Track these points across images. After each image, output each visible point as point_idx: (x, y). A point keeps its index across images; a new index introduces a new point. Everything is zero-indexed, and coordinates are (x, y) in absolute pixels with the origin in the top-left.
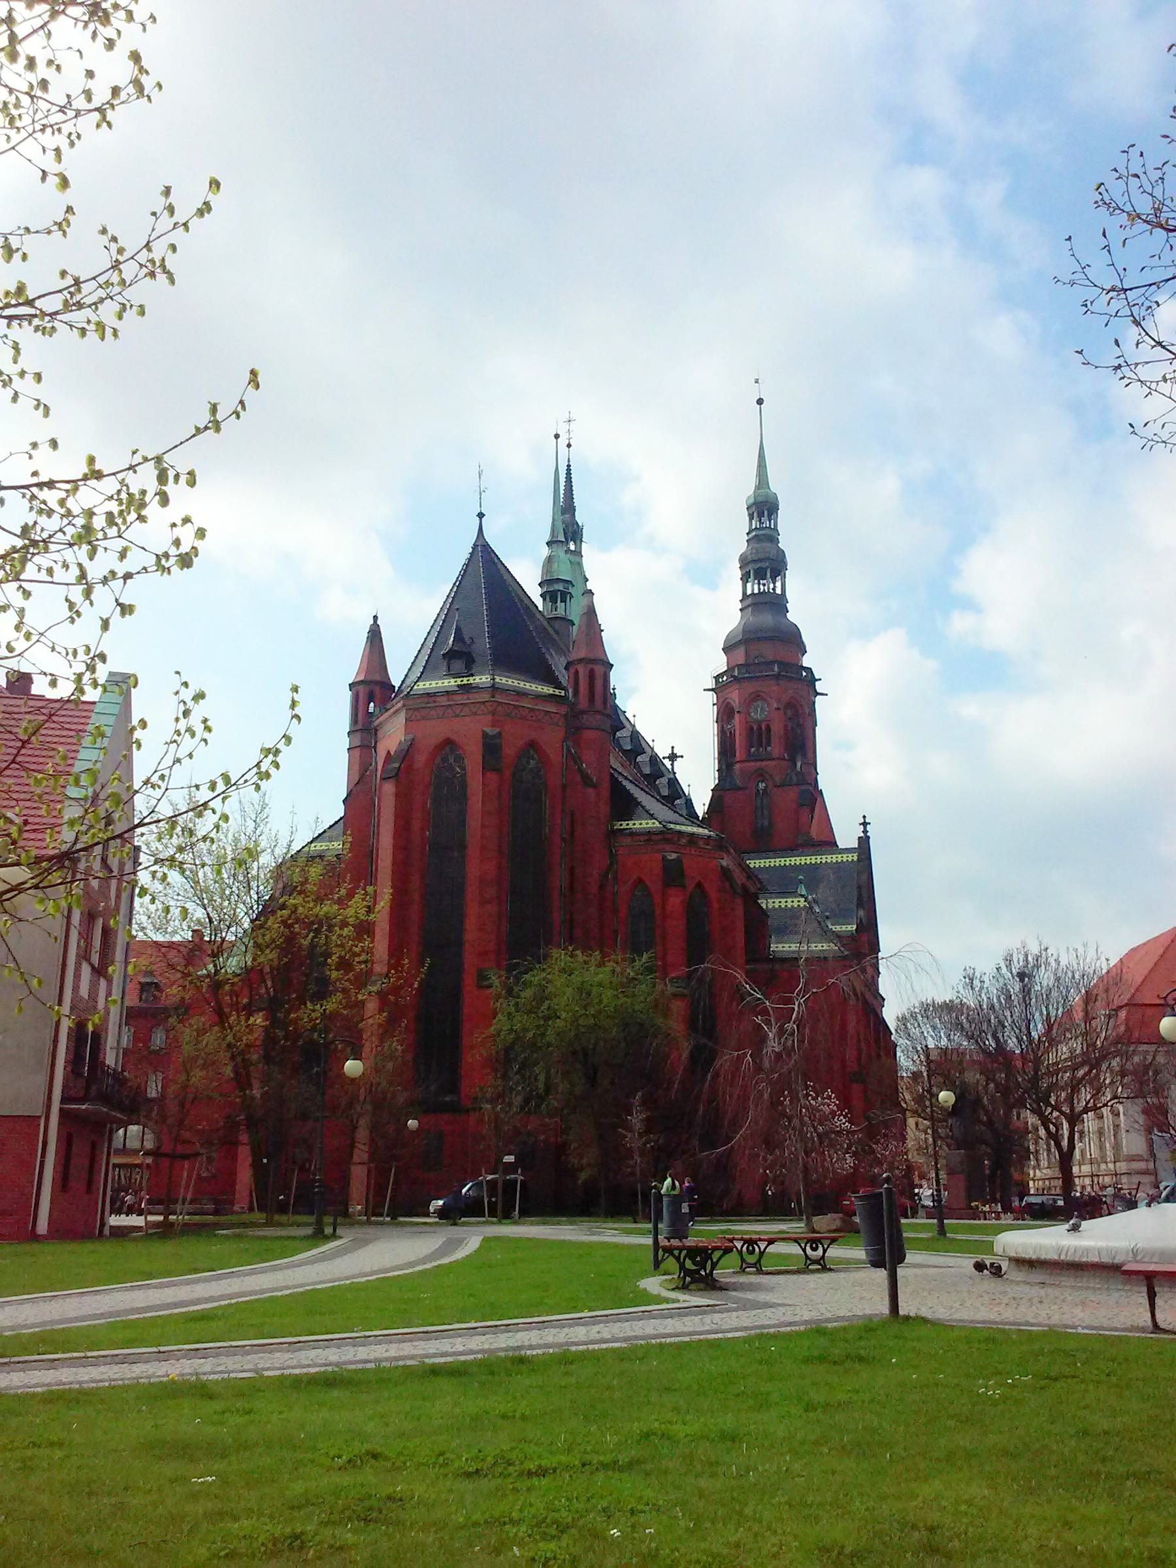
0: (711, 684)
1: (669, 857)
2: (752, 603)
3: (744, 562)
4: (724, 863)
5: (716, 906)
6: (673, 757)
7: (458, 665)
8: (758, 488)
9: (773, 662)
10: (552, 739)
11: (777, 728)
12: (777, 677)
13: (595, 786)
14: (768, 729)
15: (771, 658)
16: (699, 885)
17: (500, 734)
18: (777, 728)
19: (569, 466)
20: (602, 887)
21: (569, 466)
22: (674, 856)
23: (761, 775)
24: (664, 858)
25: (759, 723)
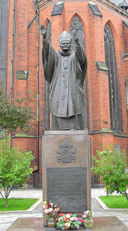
1: (57, 4)
5: (86, 24)
16: (76, 15)
22: (60, 3)
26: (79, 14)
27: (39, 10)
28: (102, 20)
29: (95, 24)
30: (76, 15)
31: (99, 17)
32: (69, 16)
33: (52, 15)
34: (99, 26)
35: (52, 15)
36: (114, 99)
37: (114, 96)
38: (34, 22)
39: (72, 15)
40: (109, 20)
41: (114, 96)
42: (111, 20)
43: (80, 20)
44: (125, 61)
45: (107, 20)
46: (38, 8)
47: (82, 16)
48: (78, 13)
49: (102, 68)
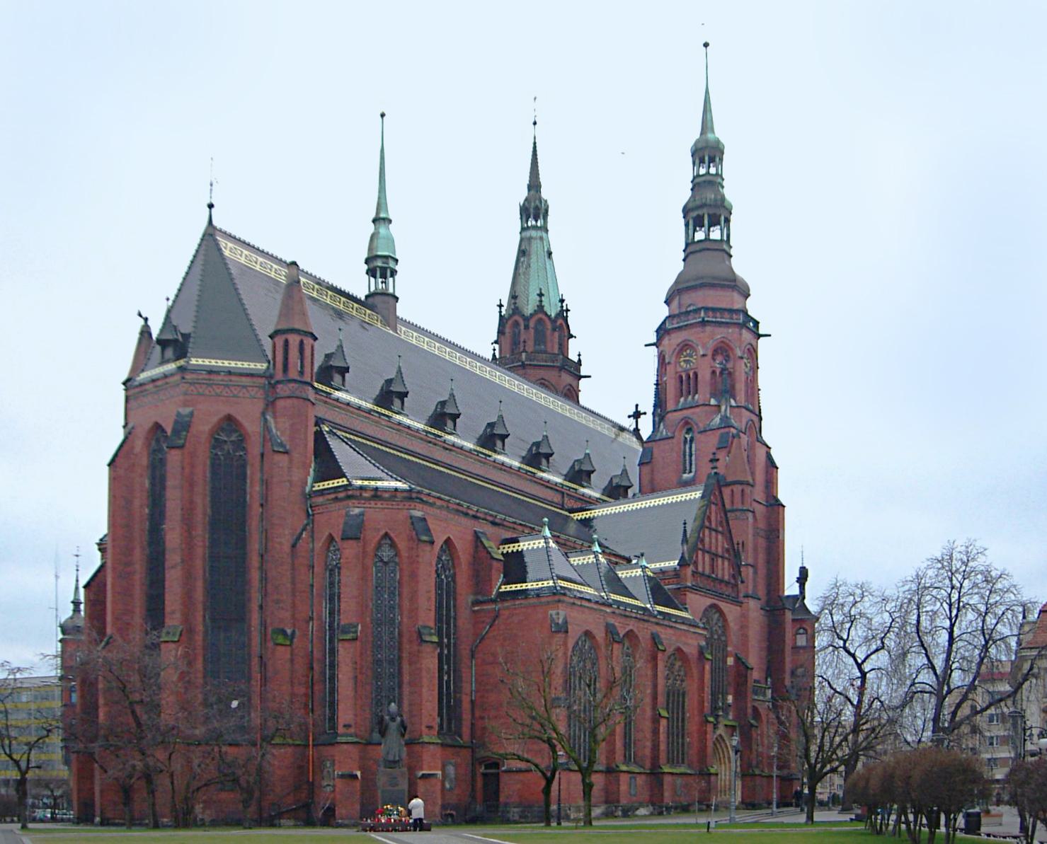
0: (654, 340)
2: (691, 249)
3: (686, 211)
4: (418, 514)
5: (404, 554)
6: (637, 415)
7: (169, 353)
8: (703, 132)
9: (697, 311)
10: (249, 413)
11: (704, 375)
12: (704, 323)
13: (286, 453)
14: (696, 375)
15: (700, 306)
17: (192, 414)
18: (704, 375)
19: (535, 143)
20: (294, 546)
21: (535, 143)
22: (357, 511)
23: (687, 423)
24: (347, 515)
25: (687, 371)
26: (392, 535)
27: (312, 511)
28: (433, 548)
29: (420, 560)
30: (386, 535)
31: (428, 544)
32: (373, 537)
33: (342, 539)
34: (428, 558)
35: (342, 539)
36: (448, 682)
37: (449, 677)
38: (304, 536)
39: (379, 537)
40: (449, 538)
41: (449, 677)
42: (452, 537)
43: (393, 545)
44: (474, 611)
45: (445, 538)
46: (311, 507)
47: (396, 540)
48: (389, 531)
49: (428, 638)
